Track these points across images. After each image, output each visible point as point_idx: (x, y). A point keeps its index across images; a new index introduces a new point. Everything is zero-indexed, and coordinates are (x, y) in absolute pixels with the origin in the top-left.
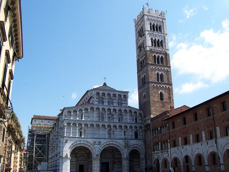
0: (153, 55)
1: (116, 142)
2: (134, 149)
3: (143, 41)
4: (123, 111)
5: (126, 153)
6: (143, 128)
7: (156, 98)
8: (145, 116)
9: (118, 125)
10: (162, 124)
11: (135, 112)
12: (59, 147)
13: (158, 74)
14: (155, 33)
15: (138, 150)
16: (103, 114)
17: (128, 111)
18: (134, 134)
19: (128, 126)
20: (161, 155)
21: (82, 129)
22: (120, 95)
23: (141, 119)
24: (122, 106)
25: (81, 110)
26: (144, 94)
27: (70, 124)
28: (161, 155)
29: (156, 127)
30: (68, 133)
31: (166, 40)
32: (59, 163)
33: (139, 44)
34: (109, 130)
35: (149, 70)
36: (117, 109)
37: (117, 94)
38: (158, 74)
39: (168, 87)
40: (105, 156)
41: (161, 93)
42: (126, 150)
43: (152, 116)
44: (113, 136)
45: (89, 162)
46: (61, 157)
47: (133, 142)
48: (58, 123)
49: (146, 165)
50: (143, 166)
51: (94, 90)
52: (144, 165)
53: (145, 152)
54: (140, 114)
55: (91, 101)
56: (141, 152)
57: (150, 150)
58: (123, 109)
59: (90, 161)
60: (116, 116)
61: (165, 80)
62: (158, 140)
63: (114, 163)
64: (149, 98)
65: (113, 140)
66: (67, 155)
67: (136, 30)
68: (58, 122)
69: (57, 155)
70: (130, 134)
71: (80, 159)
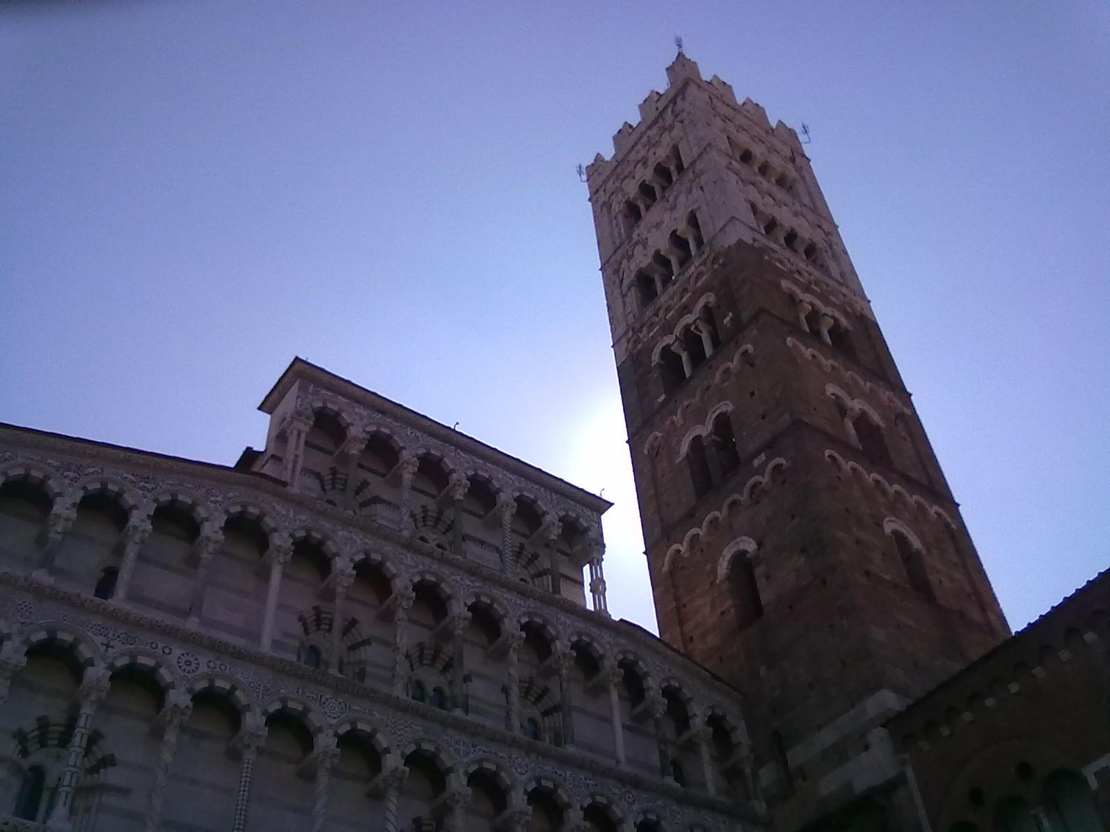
3: (682, 227)
21: (65, 740)
26: (728, 554)
29: (1025, 770)
54: (716, 722)
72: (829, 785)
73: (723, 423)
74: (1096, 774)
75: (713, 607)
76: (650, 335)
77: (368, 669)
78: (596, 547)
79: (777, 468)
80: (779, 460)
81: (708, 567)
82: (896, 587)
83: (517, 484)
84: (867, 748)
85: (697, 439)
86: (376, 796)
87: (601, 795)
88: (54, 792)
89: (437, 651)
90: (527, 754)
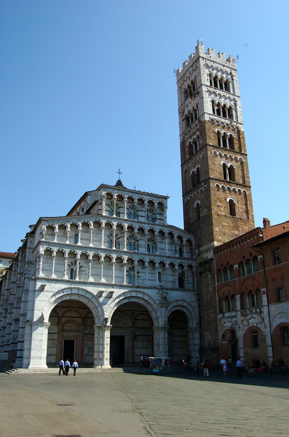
0: (216, 131)
1: (144, 294)
2: (177, 308)
4: (157, 233)
5: (163, 316)
6: (194, 269)
7: (222, 209)
8: (199, 244)
9: (147, 259)
10: (244, 257)
11: (180, 238)
12: (24, 301)
13: (224, 166)
14: (218, 92)
15: (185, 311)
16: (118, 237)
17: (166, 234)
18: (177, 278)
19: (167, 262)
20: (242, 321)
21: (75, 264)
22: (151, 203)
23: (189, 251)
24: (156, 223)
25: (75, 226)
26: (196, 203)
27: (50, 254)
28: (242, 321)
29: (228, 263)
30: (47, 270)
31: (237, 107)
32: (23, 336)
33: (186, 112)
34: (130, 268)
35: (208, 156)
36: (147, 228)
37: (147, 199)
38: (224, 166)
39: (244, 191)
40: (117, 324)
41: (231, 201)
42: (163, 310)
43: (216, 244)
44: (137, 282)
45: (84, 334)
46: (28, 321)
47: (175, 295)
48: (23, 255)
49: (201, 342)
50: (195, 345)
51: (103, 187)
52: (197, 341)
53: (200, 317)
54: (189, 241)
55: (94, 211)
56: (191, 315)
57: (211, 311)
58: (157, 229)
59: (87, 332)
60: (143, 243)
61: (238, 179)
62: (232, 291)
63: (135, 338)
64: (208, 210)
65: (139, 289)
66: (42, 318)
67: (180, 88)
68: (22, 253)
69: (17, 320)
70: (170, 278)
71: (68, 328)
72: (205, 256)
73: (198, 169)
74: (235, 267)
75: (193, 213)
76: (187, 137)
77: (120, 243)
78: (165, 208)
79: (205, 187)
80: (206, 186)
81: (193, 204)
82: (225, 216)
83: (148, 198)
84: (210, 251)
85: (193, 171)
86: (122, 266)
87: (162, 260)
88: (76, 271)
89: (133, 236)
90: (148, 256)
